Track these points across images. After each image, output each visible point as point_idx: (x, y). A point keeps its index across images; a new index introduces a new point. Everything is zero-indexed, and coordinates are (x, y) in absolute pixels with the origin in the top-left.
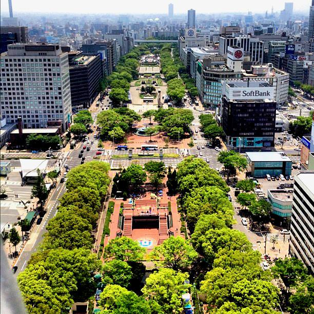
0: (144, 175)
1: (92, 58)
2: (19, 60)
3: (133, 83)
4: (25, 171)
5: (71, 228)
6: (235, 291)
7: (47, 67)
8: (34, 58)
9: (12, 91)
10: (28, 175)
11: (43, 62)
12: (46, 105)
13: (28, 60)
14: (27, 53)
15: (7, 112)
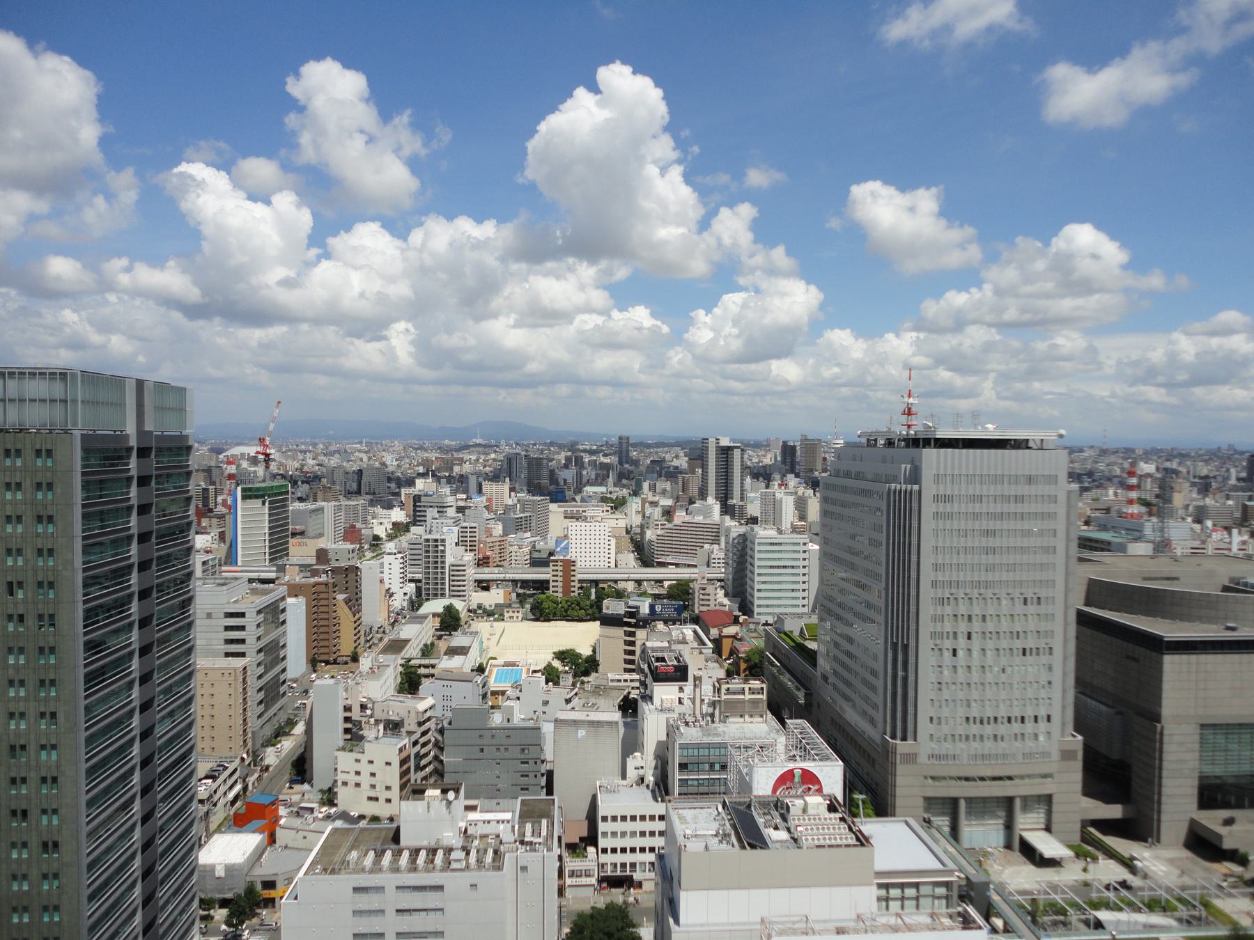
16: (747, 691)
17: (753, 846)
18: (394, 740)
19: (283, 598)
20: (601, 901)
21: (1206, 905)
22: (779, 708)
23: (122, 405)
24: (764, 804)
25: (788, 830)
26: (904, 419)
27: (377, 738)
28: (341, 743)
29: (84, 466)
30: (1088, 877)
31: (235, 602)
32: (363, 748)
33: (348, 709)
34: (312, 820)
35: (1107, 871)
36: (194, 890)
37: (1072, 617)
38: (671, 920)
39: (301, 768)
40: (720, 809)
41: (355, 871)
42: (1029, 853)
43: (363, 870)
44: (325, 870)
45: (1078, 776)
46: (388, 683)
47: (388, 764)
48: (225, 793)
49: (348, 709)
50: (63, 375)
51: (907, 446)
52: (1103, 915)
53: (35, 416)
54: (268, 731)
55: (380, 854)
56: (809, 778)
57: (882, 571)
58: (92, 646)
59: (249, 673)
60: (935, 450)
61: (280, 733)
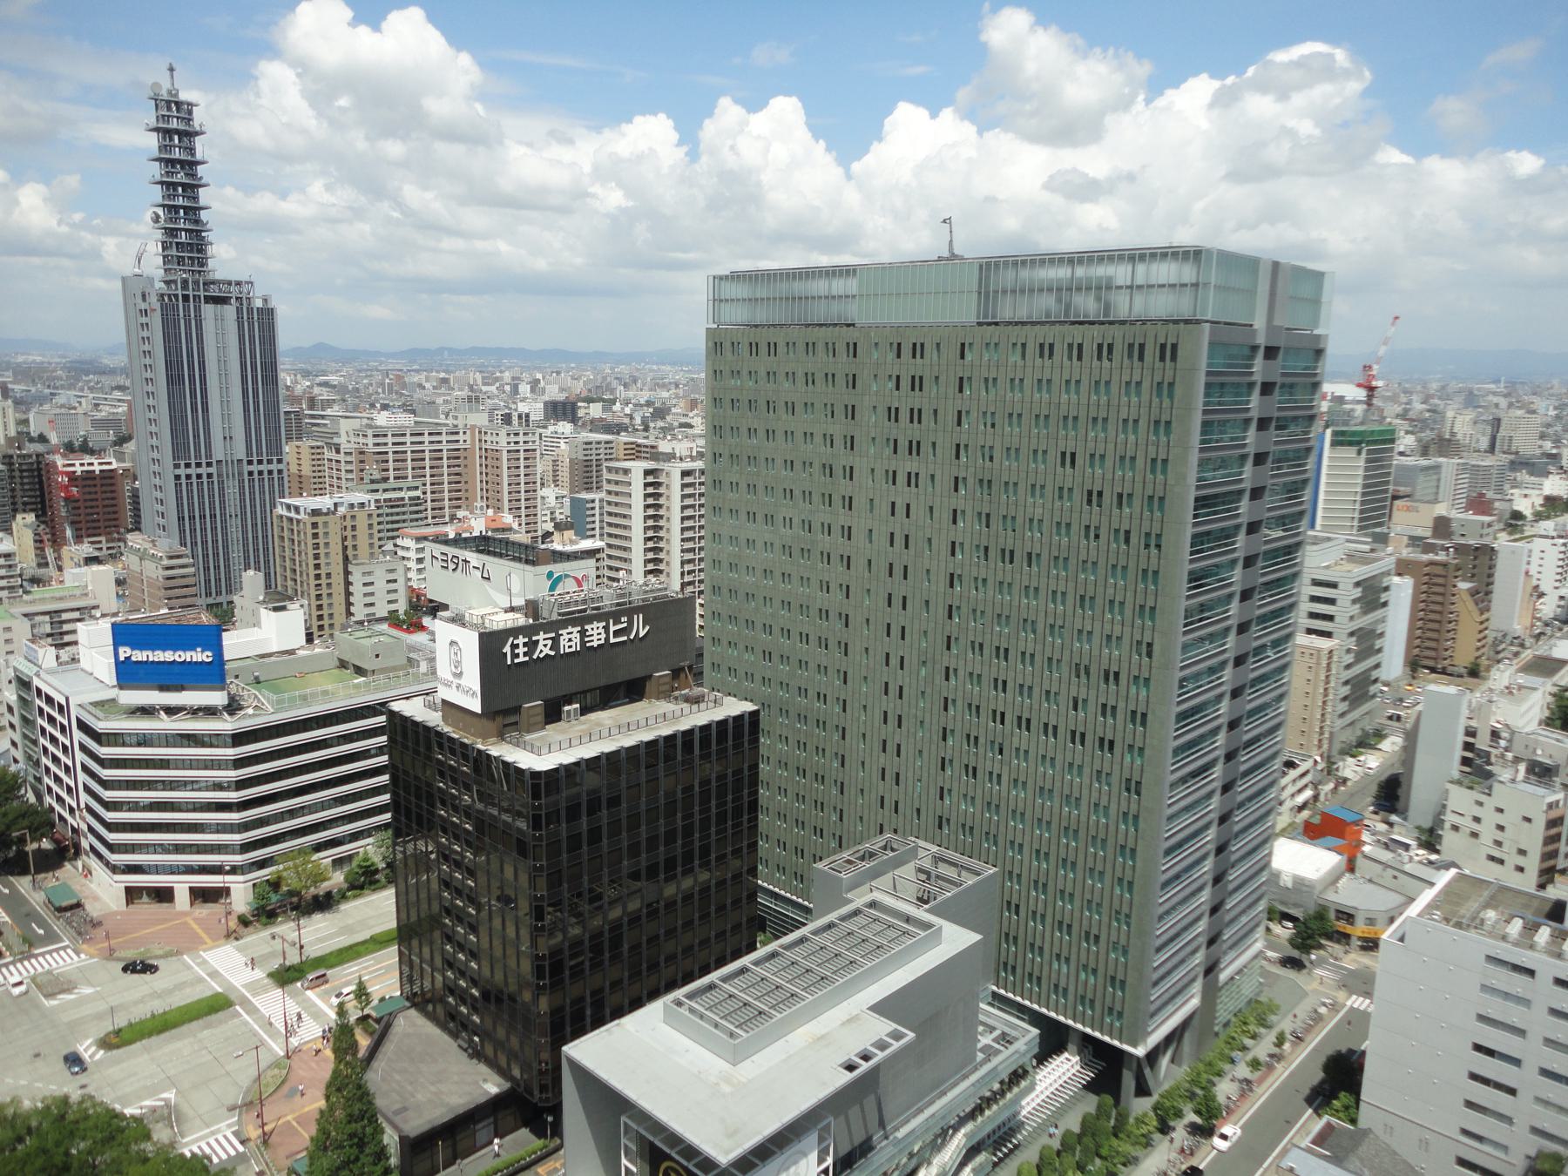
18: (1540, 791)
19: (1388, 573)
23: (1252, 292)
27: (1513, 781)
28: (1456, 775)
29: (1209, 365)
31: (1327, 567)
32: (1490, 788)
33: (1471, 733)
34: (1406, 859)
36: (1264, 888)
39: (1390, 794)
41: (1491, 934)
43: (1504, 938)
44: (1447, 920)
46: (1531, 714)
47: (1528, 820)
48: (1293, 795)
49: (1471, 733)
50: (1194, 255)
53: (1161, 306)
54: (1351, 736)
55: (1531, 928)
58: (1196, 579)
59: (1335, 659)
61: (1367, 742)
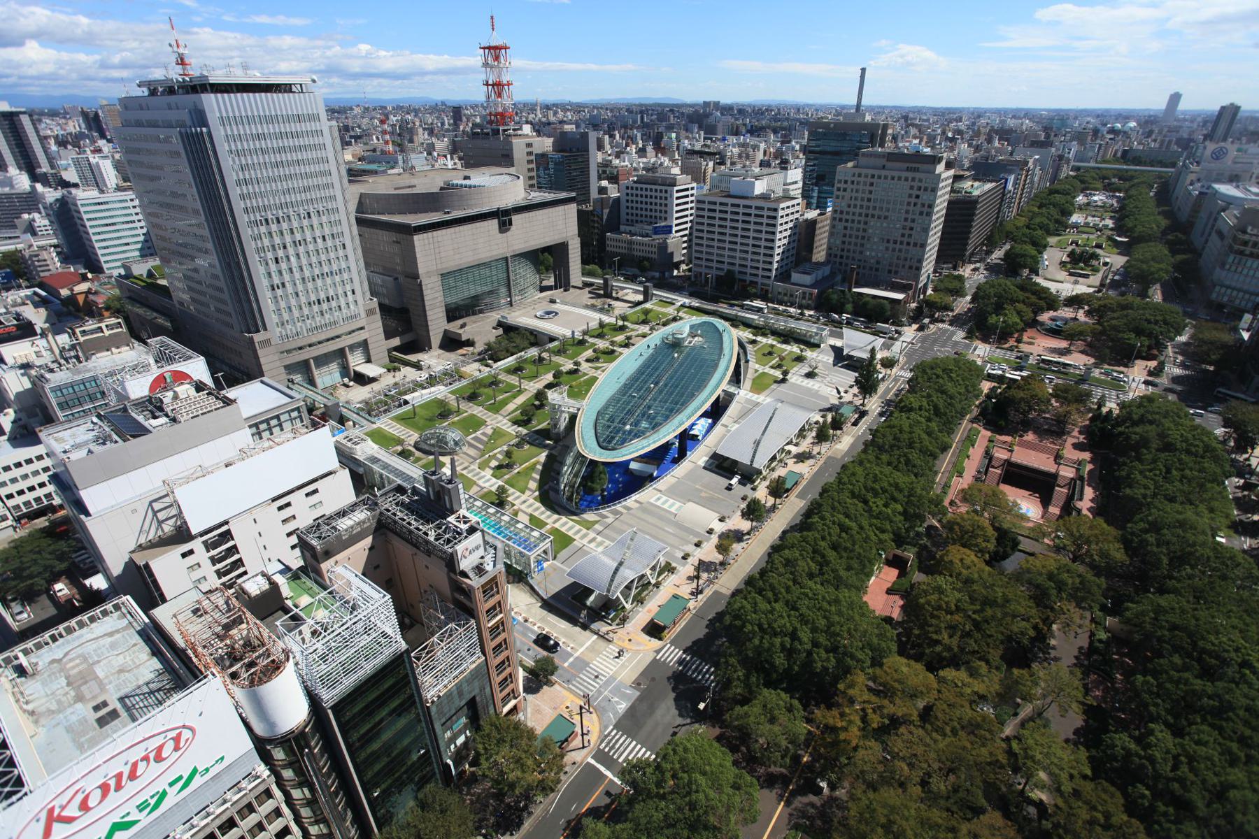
0: (1049, 401)
1: (989, 186)
2: (873, 176)
3: (1052, 240)
4: (849, 346)
5: (910, 446)
6: (1209, 647)
7: (915, 192)
8: (896, 174)
9: (849, 225)
10: (852, 353)
11: (910, 183)
12: (897, 253)
13: (886, 177)
14: (889, 165)
15: (836, 256)
16: (104, 329)
17: (134, 437)
20: (22, 533)
21: (457, 371)
22: (138, 332)
24: (142, 404)
25: (167, 415)
26: (179, 69)
30: (397, 379)
35: (408, 373)
37: (353, 221)
38: (82, 517)
40: (95, 420)
42: (361, 379)
45: (380, 324)
51: (188, 93)
52: (406, 397)
56: (181, 377)
57: (198, 206)
60: (212, 95)
